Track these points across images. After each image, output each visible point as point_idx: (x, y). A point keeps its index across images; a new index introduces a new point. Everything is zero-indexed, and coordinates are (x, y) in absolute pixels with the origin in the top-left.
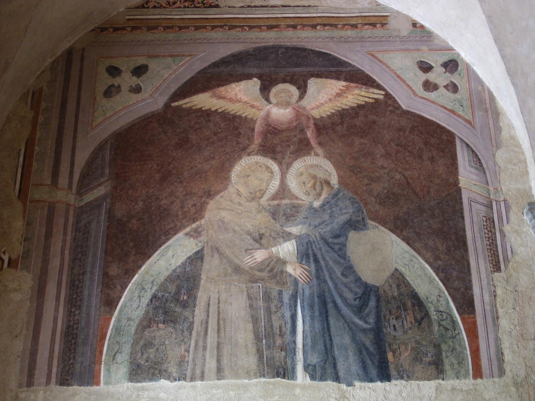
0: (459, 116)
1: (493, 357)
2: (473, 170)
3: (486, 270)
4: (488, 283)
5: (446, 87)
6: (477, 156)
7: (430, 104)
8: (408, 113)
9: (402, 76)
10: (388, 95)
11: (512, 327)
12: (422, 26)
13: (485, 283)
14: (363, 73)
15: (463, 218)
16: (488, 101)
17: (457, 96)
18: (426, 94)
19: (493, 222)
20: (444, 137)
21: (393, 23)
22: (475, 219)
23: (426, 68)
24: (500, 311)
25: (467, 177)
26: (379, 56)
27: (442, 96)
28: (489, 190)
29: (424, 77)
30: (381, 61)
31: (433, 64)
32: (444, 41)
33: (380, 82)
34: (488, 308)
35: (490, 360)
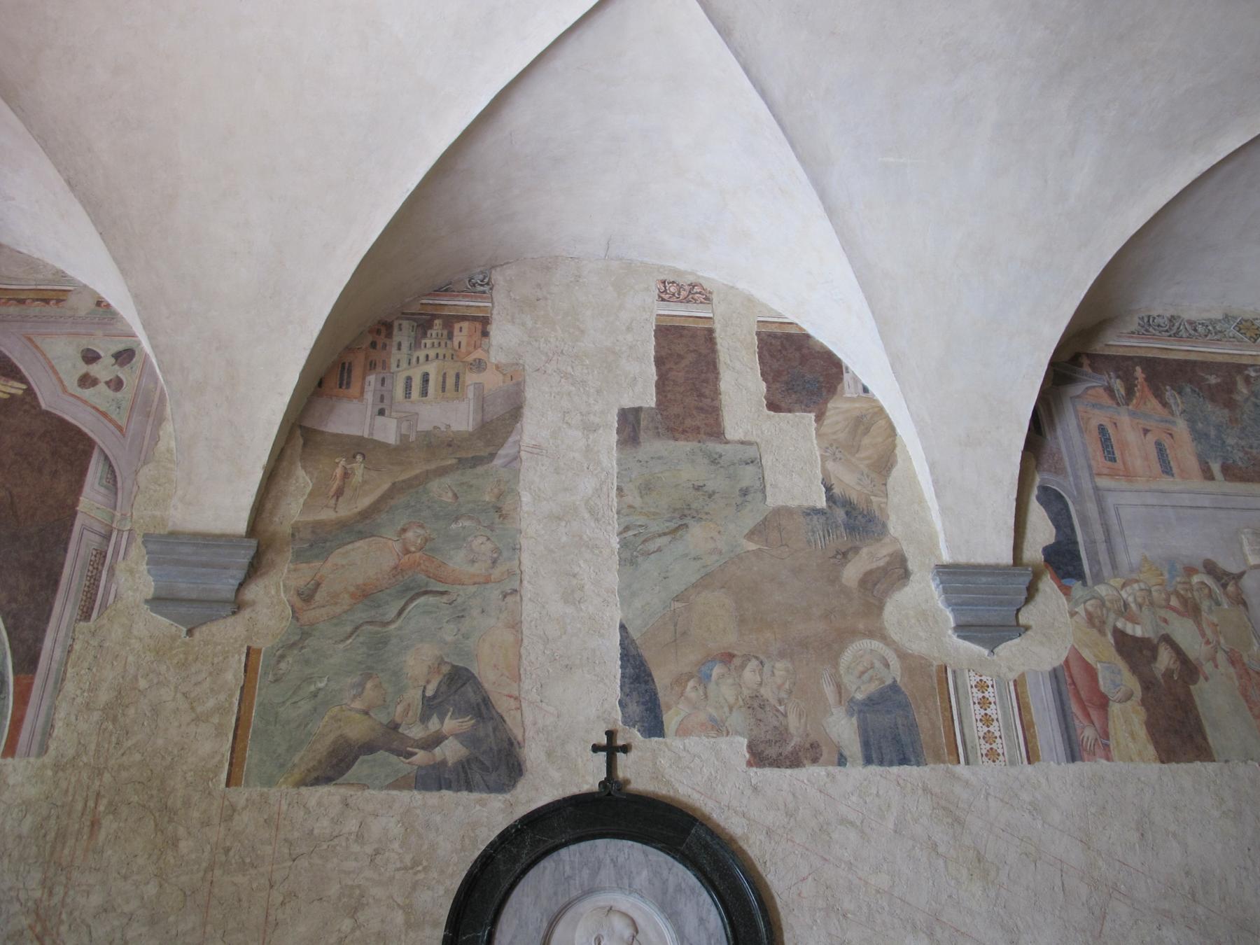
0: (111, 421)
1: (39, 730)
2: (102, 490)
3: (71, 617)
4: (67, 635)
5: (107, 383)
6: (113, 472)
7: (79, 403)
8: (47, 413)
9: (57, 368)
10: (30, 391)
11: (79, 692)
12: (108, 305)
13: (62, 634)
14: (9, 360)
15: (66, 550)
16: (154, 406)
17: (119, 395)
18: (79, 392)
19: (105, 557)
20: (81, 447)
21: (72, 300)
22: (82, 552)
23: (90, 357)
24: (70, 670)
25: (92, 498)
26: (38, 340)
27: (100, 395)
28: (114, 516)
29: (83, 368)
30: (37, 347)
31: (102, 354)
32: (128, 325)
33: (26, 374)
34: (55, 666)
35: (33, 733)
